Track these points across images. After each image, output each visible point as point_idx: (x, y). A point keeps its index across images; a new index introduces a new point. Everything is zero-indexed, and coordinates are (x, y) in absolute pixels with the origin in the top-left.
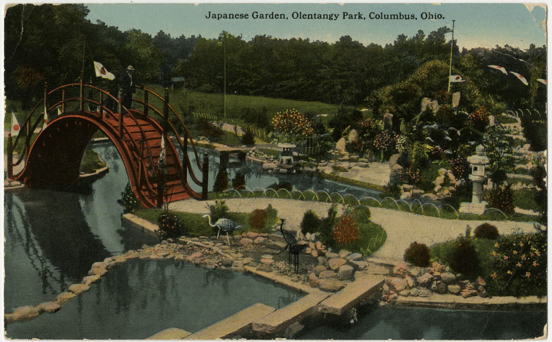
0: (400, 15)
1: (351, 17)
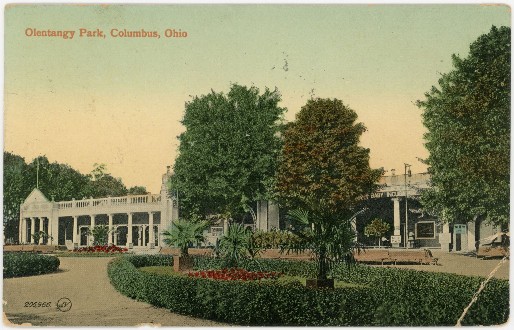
0: (143, 32)
1: (90, 34)
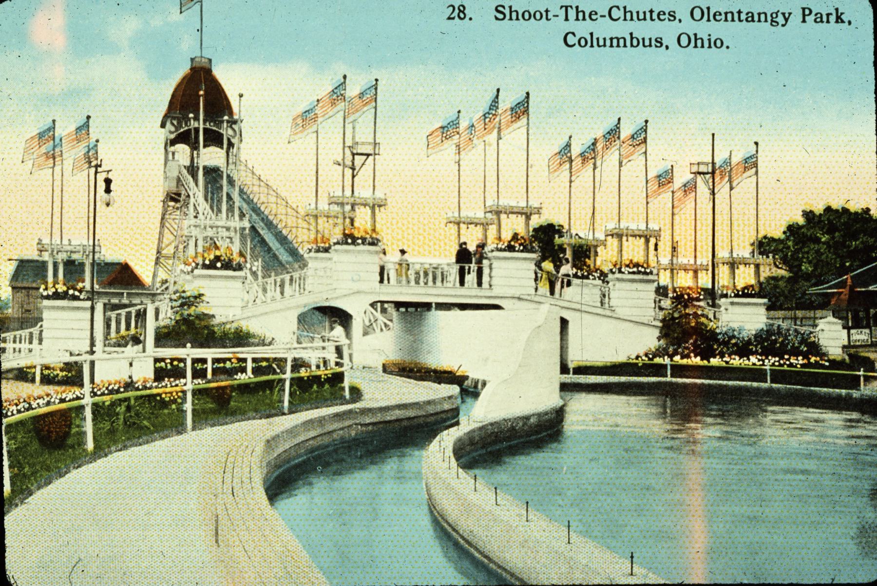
0: (632, 38)
1: (819, 19)
